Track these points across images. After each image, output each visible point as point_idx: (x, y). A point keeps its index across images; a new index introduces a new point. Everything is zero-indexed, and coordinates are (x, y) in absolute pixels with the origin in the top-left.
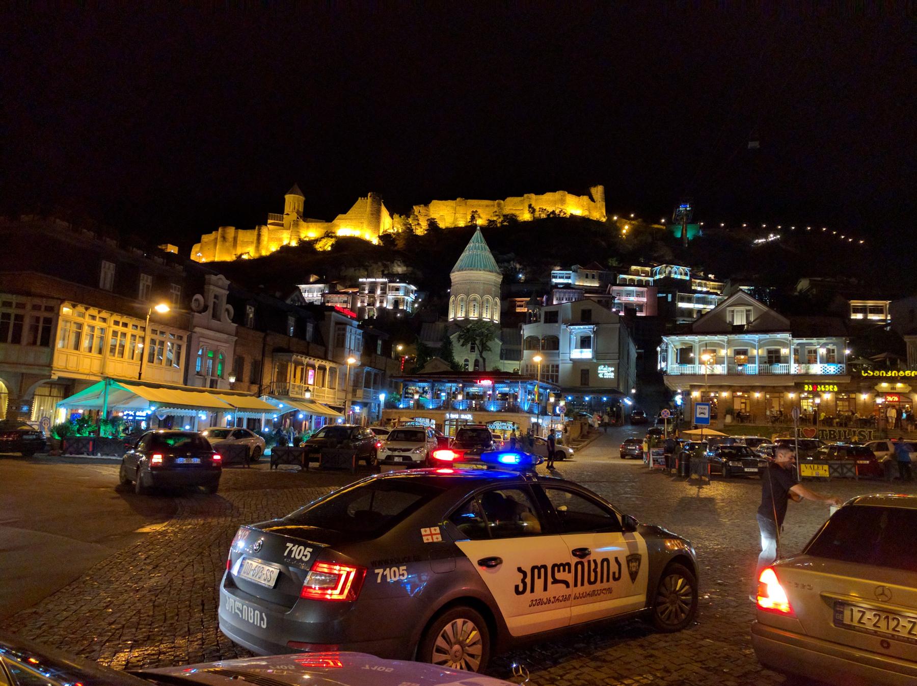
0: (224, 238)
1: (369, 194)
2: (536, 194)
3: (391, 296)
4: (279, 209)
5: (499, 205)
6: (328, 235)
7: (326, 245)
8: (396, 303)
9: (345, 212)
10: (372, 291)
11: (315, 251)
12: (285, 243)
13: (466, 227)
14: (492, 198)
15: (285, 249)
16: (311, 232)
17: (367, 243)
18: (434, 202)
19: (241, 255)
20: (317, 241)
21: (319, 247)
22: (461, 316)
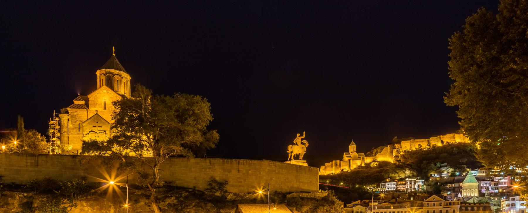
0: (336, 164)
3: (417, 184)
4: (347, 151)
6: (374, 161)
7: (375, 164)
8: (418, 186)
10: (411, 183)
11: (371, 168)
13: (417, 150)
14: (425, 138)
15: (360, 167)
16: (368, 160)
17: (390, 163)
18: (402, 142)
20: (371, 163)
21: (372, 165)
22: (468, 195)
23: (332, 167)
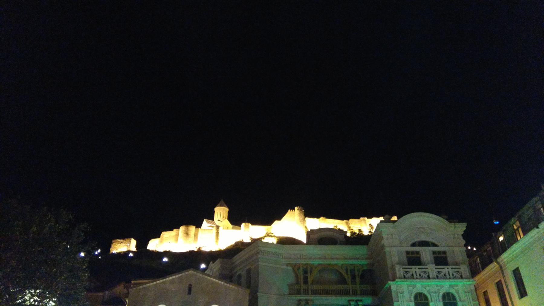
0: (187, 234)
1: (296, 208)
2: (368, 218)
4: (211, 217)
5: (347, 223)
9: (280, 218)
12: (238, 239)
19: (199, 248)
20: (262, 238)
23: (177, 239)
